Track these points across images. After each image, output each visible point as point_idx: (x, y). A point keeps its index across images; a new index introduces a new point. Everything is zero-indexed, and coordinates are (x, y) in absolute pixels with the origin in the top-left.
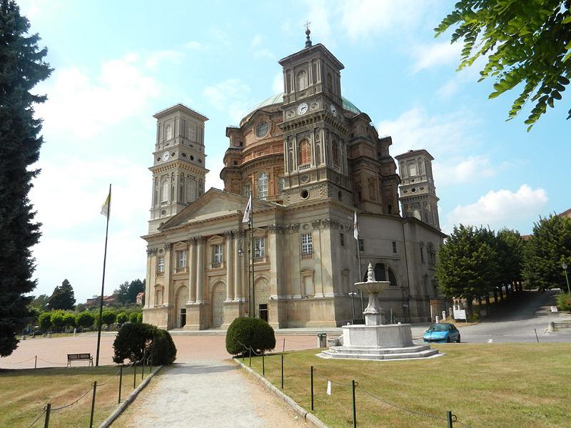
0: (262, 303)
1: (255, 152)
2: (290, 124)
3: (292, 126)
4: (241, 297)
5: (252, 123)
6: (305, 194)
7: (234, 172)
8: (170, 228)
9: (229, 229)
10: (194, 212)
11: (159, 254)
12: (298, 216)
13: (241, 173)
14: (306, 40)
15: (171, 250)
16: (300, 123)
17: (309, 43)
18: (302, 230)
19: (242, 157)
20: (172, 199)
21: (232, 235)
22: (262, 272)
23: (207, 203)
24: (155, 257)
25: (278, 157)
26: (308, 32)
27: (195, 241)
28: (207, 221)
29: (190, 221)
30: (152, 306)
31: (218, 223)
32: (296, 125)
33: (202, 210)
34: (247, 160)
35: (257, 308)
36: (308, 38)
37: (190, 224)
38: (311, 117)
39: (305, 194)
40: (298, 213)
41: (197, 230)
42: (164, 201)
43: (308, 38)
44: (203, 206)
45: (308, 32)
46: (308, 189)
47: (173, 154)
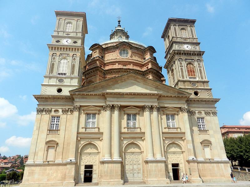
0: (173, 162)
1: (119, 64)
2: (182, 52)
3: (182, 54)
6: (196, 94)
8: (81, 93)
11: (53, 113)
12: (194, 105)
13: (105, 74)
16: (188, 54)
19: (105, 65)
20: (73, 72)
23: (122, 82)
25: (137, 71)
26: (119, 22)
27: (113, 107)
28: (127, 94)
29: (108, 91)
30: (39, 161)
31: (137, 98)
32: (185, 54)
33: (116, 86)
34: (107, 68)
37: (107, 94)
38: (196, 53)
39: (196, 94)
40: (194, 104)
41: (115, 99)
42: (61, 72)
45: (119, 22)
46: (199, 91)
47: (75, 42)
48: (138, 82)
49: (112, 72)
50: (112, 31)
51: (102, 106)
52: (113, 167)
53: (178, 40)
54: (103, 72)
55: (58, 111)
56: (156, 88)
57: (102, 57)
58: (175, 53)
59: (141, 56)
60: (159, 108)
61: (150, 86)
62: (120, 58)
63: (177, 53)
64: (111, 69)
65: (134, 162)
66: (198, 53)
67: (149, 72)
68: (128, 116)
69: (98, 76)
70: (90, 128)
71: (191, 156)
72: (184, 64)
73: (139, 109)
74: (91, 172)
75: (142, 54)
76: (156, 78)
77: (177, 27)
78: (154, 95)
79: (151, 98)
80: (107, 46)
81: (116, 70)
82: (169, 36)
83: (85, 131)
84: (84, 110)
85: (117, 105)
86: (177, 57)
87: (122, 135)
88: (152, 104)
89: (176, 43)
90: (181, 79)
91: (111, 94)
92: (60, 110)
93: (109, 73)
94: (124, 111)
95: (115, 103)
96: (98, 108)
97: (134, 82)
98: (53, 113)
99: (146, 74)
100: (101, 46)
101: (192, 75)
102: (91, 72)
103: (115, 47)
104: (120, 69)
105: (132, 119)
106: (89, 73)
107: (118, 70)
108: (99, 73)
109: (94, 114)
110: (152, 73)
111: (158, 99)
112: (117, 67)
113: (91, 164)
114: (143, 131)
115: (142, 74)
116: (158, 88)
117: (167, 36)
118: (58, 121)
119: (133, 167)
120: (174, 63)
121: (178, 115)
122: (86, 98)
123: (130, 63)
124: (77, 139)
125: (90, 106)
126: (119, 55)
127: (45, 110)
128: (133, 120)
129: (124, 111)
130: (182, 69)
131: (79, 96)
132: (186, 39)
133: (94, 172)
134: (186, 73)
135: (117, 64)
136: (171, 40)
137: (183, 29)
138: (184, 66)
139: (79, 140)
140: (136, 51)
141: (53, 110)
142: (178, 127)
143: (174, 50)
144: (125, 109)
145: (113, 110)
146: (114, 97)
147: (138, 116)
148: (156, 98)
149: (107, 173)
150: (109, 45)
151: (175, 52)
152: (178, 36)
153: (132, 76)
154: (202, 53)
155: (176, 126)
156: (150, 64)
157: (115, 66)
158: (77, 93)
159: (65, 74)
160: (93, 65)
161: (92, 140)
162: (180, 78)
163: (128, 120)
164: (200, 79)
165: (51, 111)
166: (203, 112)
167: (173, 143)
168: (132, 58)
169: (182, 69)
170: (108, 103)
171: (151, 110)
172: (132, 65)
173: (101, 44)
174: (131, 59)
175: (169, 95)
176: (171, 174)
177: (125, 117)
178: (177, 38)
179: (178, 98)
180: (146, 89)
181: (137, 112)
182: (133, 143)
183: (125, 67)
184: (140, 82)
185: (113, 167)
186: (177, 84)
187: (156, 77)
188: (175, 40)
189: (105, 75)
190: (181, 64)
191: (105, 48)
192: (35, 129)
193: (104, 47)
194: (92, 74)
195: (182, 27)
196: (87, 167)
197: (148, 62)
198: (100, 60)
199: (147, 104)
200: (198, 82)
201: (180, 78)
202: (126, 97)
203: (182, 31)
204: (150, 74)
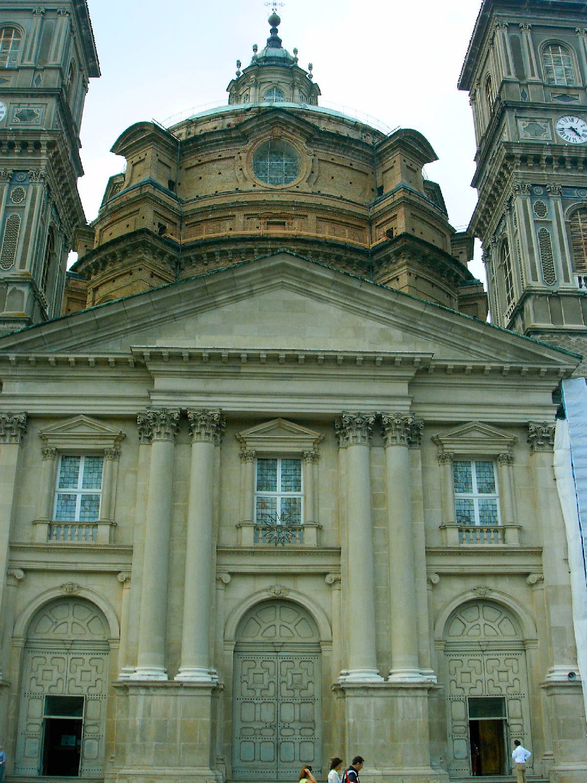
1: (249, 217)
2: (547, 153)
3: (549, 160)
4: (420, 663)
5: (244, 138)
7: (162, 254)
9: (370, 408)
10: (174, 317)
13: (178, 266)
14: (269, 35)
15: (22, 443)
17: (275, 41)
22: (490, 583)
23: (238, 298)
26: (275, 21)
32: (562, 161)
35: (459, 712)
36: (274, 31)
37: (157, 356)
43: (274, 31)
44: (216, 306)
45: (275, 21)
48: (319, 298)
49: (211, 256)
50: (239, 64)
51: (131, 419)
52: (175, 706)
53: (533, 95)
54: (172, 258)
56: (405, 329)
57: (172, 184)
58: (510, 157)
59: (364, 177)
60: (415, 427)
61: (377, 318)
62: (257, 188)
63: (524, 159)
64: (207, 243)
65: (285, 692)
67: (397, 254)
68: (261, 469)
69: (146, 275)
70: (73, 525)
71: (562, 663)
72: (557, 211)
73: (314, 434)
74: (76, 728)
75: (368, 170)
76: (433, 285)
77: (526, 37)
78: (389, 362)
79: (374, 378)
80: (197, 131)
81: (233, 247)
82: (489, 80)
83: (50, 536)
84: (43, 438)
85: (204, 412)
86: (518, 173)
87: (227, 560)
88: (379, 409)
89: (520, 108)
90: (539, 285)
91: (176, 357)
93: (199, 258)
94: (241, 441)
96: (113, 429)
97: (298, 297)
99: (380, 263)
100: (168, 133)
102: (113, 256)
104: (253, 239)
105: (279, 483)
106: (105, 263)
107: (241, 246)
108: (148, 258)
110: (414, 254)
111: (412, 384)
112: (239, 232)
113: (74, 691)
114: (330, 540)
115: (361, 264)
116: (416, 331)
117: (483, 81)
119: (277, 714)
120: (510, 209)
121: (510, 460)
122: (57, 379)
123: (302, 209)
124: (9, 575)
125: (75, 420)
126: (249, 172)
130: (544, 238)
131: (22, 371)
133: (89, 731)
134: (562, 257)
135: (240, 218)
136: (499, 99)
137: (555, 45)
138: (555, 223)
139: (20, 581)
140: (335, 155)
142: (509, 520)
143: (508, 145)
144: (246, 433)
145: (184, 436)
146: (191, 375)
147: (309, 466)
148: (400, 379)
149: (143, 739)
150: (209, 127)
151: (515, 151)
152: (530, 78)
153: (288, 266)
155: (499, 519)
156: (401, 212)
157: (228, 224)
158: (12, 356)
160: (125, 222)
162: (535, 279)
163: (260, 488)
167: (483, 602)
168: (318, 188)
169: (544, 238)
170: (160, 401)
171: (377, 440)
172: (312, 217)
173: (165, 125)
174: (310, 191)
175: (470, 361)
176: (462, 747)
178: (526, 85)
179: (516, 376)
180: (358, 332)
181: (307, 447)
182: (278, 602)
183: (276, 231)
184: (327, 301)
185: (175, 706)
186: (519, 311)
187: (430, 278)
188: (514, 94)
189: (183, 269)
190: (540, 210)
191: (187, 142)
193: (182, 135)
194: (118, 266)
195: (547, 36)
196: (55, 703)
197: (394, 207)
198: (156, 200)
199: (352, 407)
201: (535, 279)
202: (251, 376)
203: (550, 54)
204: (401, 262)
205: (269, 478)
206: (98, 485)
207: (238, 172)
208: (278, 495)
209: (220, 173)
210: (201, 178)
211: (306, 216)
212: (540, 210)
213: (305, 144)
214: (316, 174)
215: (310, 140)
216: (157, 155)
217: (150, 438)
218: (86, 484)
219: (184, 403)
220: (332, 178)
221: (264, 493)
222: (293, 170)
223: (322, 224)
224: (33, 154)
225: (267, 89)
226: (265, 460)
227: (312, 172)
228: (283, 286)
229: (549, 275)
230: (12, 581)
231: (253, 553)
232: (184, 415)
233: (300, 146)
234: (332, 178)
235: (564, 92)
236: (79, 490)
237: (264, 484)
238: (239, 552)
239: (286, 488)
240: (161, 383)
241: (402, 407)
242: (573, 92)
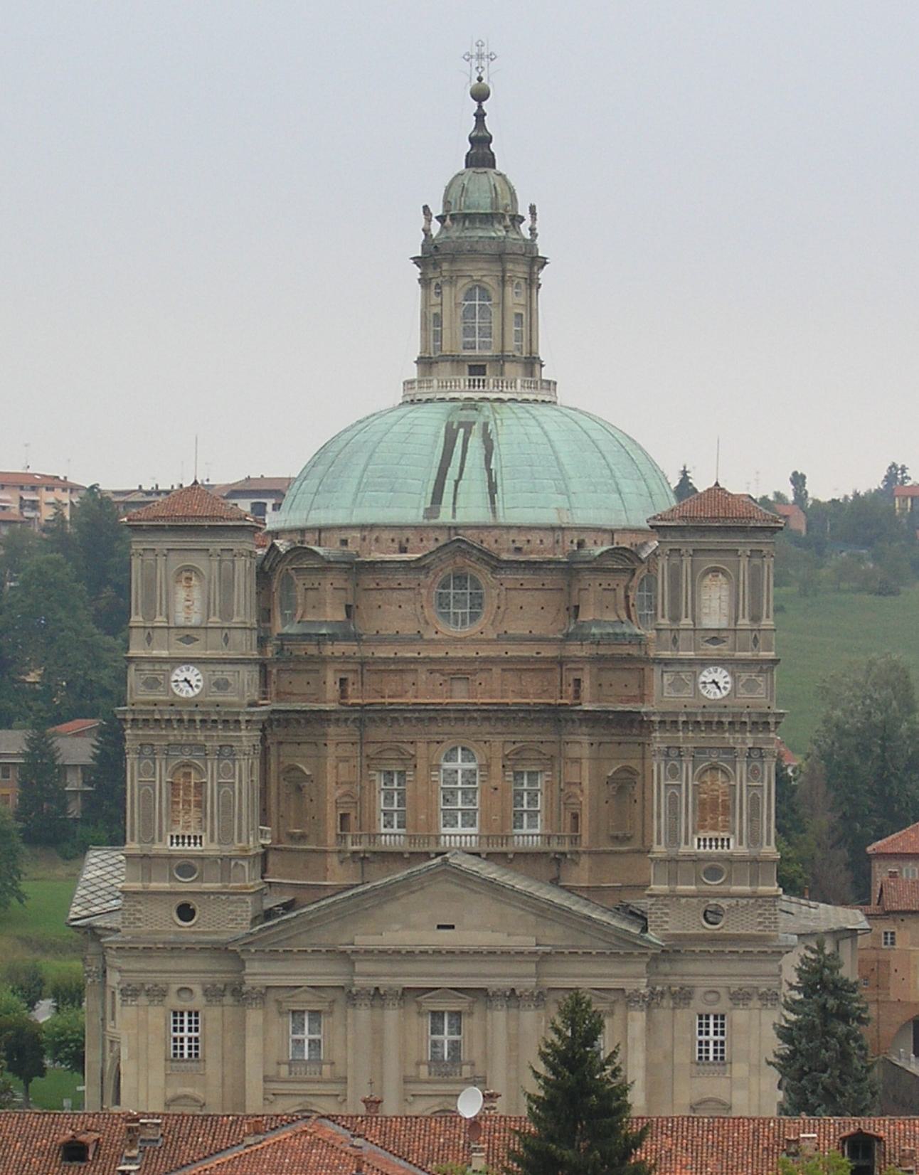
9: (509, 983)
11: (173, 1001)
16: (709, 723)
18: (698, 1005)
21: (512, 997)
24: (160, 1010)
26: (480, 95)
43: (480, 116)
45: (480, 95)
49: (395, 720)
55: (191, 991)
66: (755, 719)
68: (433, 1019)
81: (417, 715)
87: (410, 1087)
92: (198, 990)
93: (383, 720)
94: (419, 1004)
95: (384, 982)
97: (458, 890)
98: (173, 1001)
101: (714, 828)
103: (412, 565)
109: (316, 1014)
111: (537, 963)
118: (193, 1026)
122: (284, 960)
126: (430, 613)
127: (149, 990)
128: (451, 1033)
129: (419, 1004)
132: (716, 638)
141: (175, 987)
154: (772, 720)
159: (195, 837)
161: (312, 1100)
164: (743, 850)
165: (164, 993)
166: (725, 997)
170: (360, 981)
177: (428, 1022)
184: (480, 893)
190: (674, 772)
192: (127, 1058)
200: (729, 860)
205: (439, 1025)
206: (319, 1032)
207: (419, 610)
208: (446, 1038)
209: (400, 607)
210: (380, 607)
211: (491, 670)
212: (674, 772)
213: (489, 576)
214: (502, 609)
215: (495, 569)
216: (332, 584)
217: (355, 1005)
218: (310, 1032)
219: (375, 982)
220: (521, 608)
221: (436, 1037)
222: (477, 601)
223: (508, 675)
224: (234, 730)
225: (465, 289)
226: (437, 1015)
227: (499, 608)
228: (447, 881)
229: (673, 839)
230: (267, 1102)
231: (428, 1082)
232: (377, 989)
233: (486, 577)
234: (521, 608)
235: (714, 634)
236: (306, 1036)
237: (436, 1030)
238: (418, 1081)
239: (451, 1033)
240: (359, 967)
241: (530, 983)
242: (724, 634)
